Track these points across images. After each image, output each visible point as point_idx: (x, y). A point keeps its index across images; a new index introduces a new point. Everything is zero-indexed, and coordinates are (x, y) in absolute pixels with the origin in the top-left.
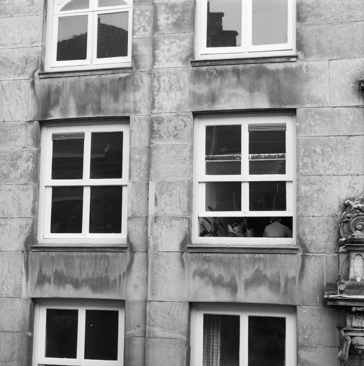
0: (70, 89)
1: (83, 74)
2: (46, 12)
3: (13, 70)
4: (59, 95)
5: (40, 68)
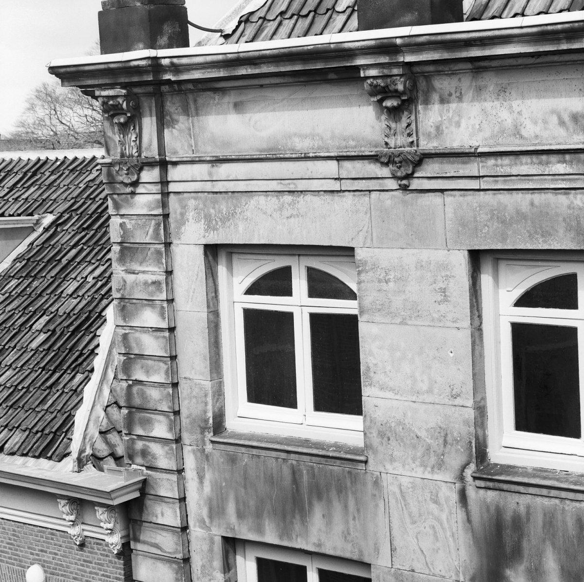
0: (544, 527)
1: (571, 495)
2: (480, 317)
3: (419, 454)
4: (522, 535)
5: (474, 460)
